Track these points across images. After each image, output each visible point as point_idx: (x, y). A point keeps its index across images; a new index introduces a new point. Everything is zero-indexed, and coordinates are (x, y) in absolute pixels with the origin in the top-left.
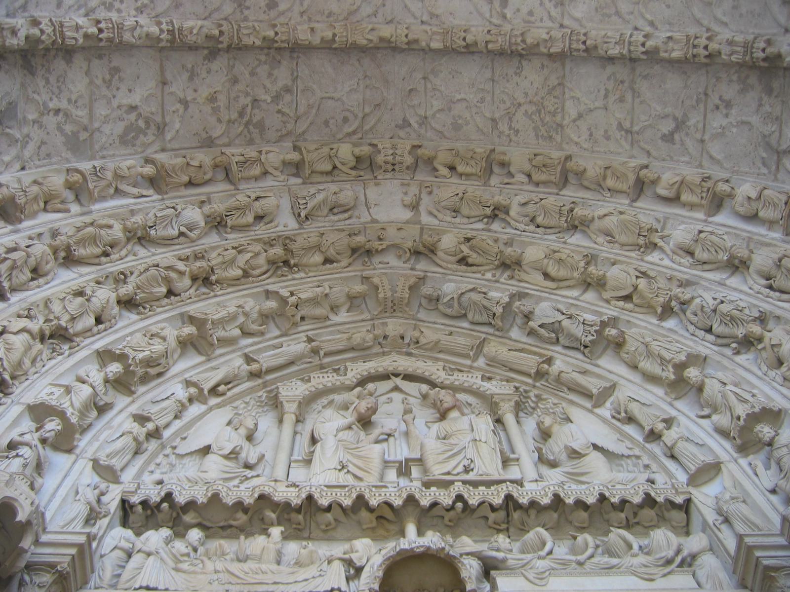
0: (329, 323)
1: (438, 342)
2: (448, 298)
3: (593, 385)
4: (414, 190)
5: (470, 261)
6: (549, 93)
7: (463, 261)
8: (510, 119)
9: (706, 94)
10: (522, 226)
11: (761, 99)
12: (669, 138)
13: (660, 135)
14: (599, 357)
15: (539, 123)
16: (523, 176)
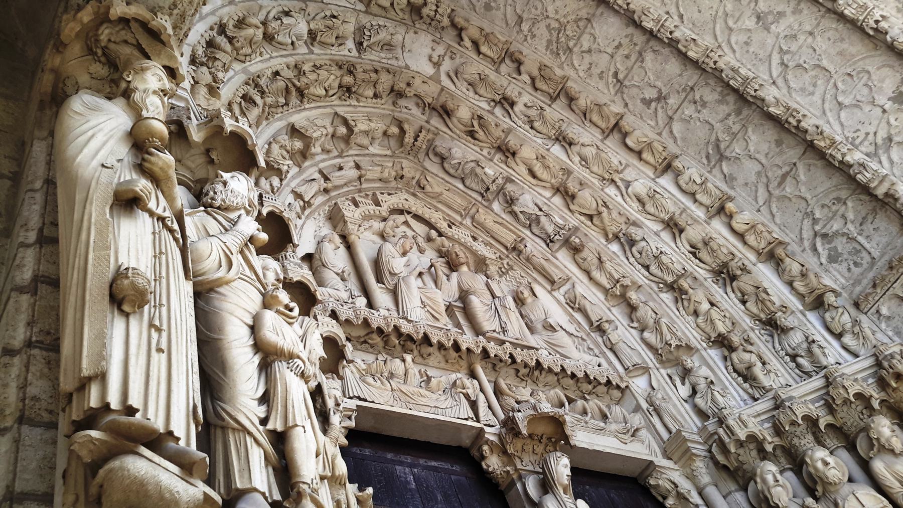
0: (367, 152)
1: (441, 194)
2: (456, 161)
3: (556, 274)
4: (440, 50)
5: (477, 136)
6: (576, 21)
7: (472, 134)
8: (534, 23)
9: (692, 89)
10: (520, 123)
11: (729, 115)
12: (647, 103)
13: (642, 96)
14: (557, 251)
15: (554, 39)
16: (528, 78)
